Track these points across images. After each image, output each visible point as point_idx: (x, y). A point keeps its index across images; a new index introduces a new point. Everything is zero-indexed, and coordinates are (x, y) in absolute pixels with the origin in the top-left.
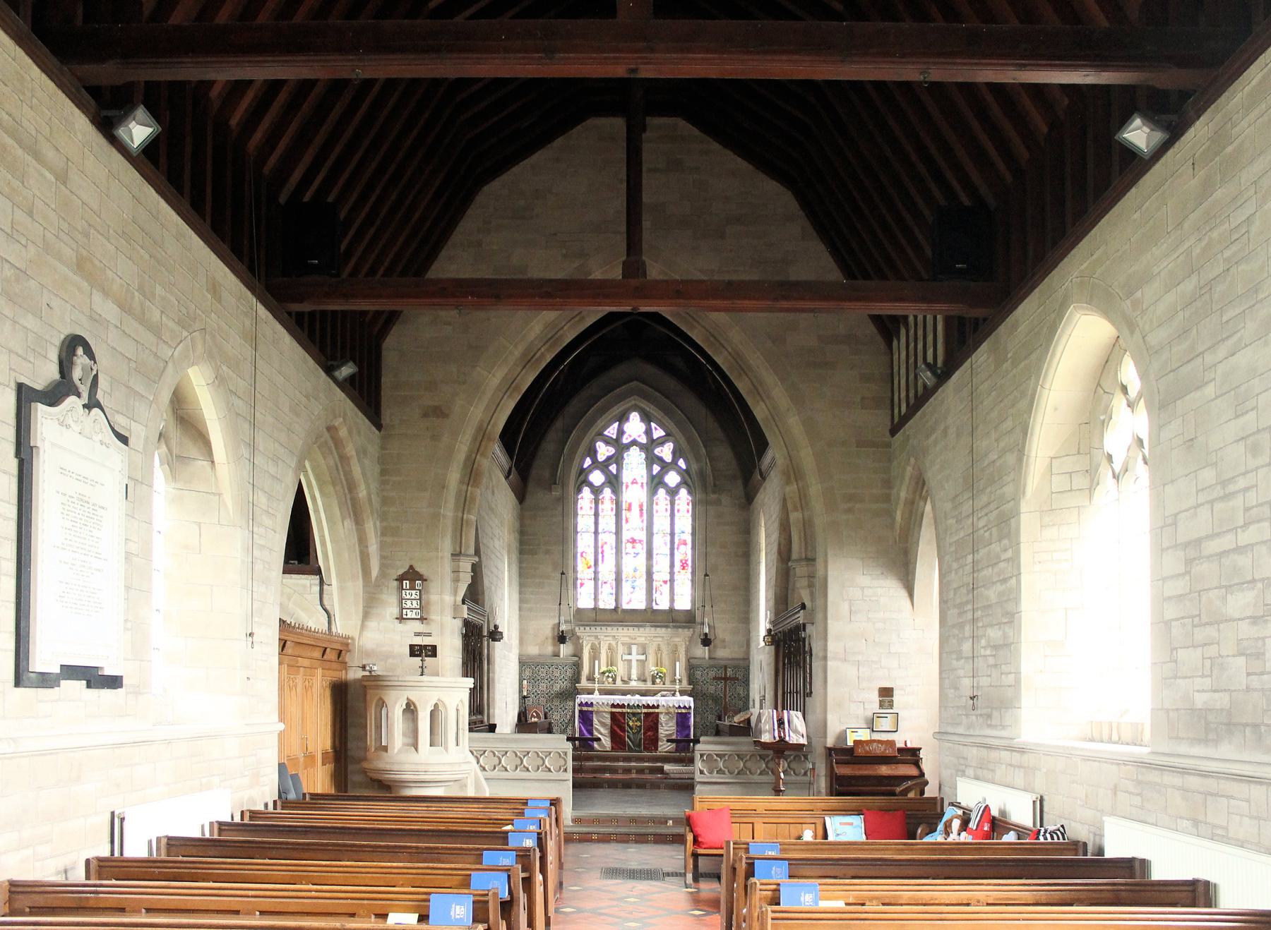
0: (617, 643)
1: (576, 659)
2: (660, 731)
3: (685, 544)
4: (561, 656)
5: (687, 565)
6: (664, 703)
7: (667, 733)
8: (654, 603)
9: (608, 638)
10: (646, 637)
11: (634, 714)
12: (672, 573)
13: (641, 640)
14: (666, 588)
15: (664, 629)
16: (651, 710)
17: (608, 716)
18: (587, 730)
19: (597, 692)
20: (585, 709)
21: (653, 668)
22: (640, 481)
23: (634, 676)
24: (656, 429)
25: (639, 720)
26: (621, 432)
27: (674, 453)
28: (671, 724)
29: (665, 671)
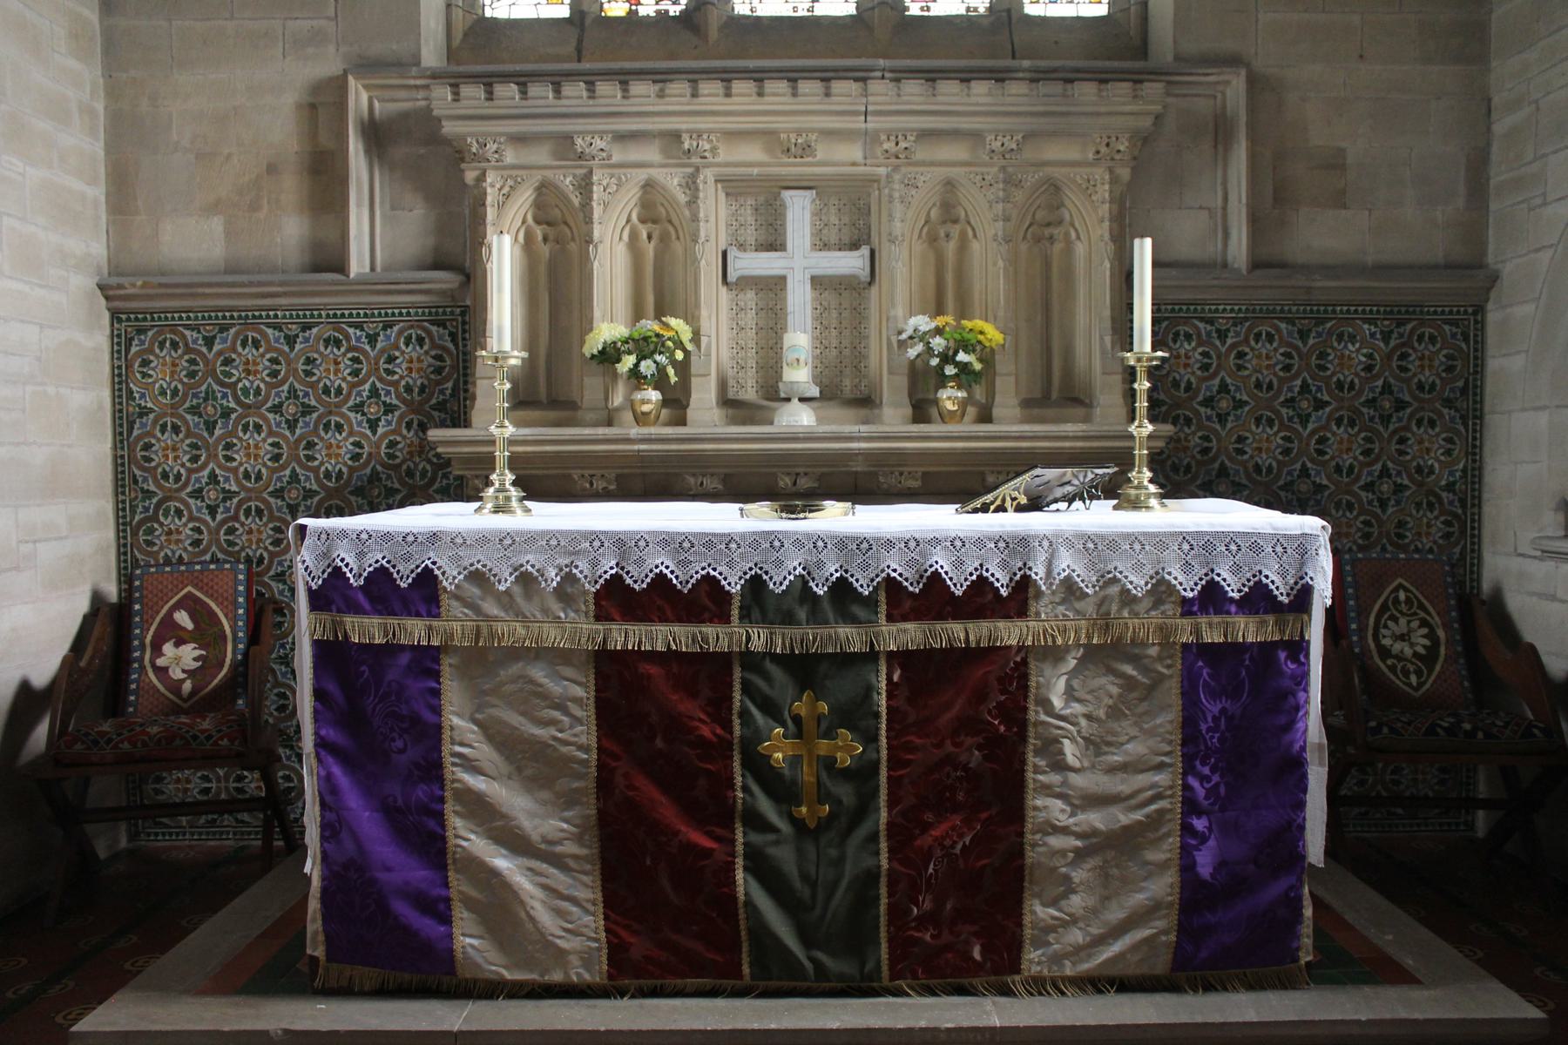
0: (691, 185)
1: (445, 280)
2: (1046, 808)
4: (358, 265)
6: (1067, 563)
9: (635, 153)
10: (870, 139)
13: (845, 157)
16: (958, 632)
17: (578, 689)
18: (392, 814)
19: (503, 477)
20: (367, 628)
21: (923, 323)
23: (799, 376)
25: (854, 715)
28: (1136, 749)
29: (993, 334)
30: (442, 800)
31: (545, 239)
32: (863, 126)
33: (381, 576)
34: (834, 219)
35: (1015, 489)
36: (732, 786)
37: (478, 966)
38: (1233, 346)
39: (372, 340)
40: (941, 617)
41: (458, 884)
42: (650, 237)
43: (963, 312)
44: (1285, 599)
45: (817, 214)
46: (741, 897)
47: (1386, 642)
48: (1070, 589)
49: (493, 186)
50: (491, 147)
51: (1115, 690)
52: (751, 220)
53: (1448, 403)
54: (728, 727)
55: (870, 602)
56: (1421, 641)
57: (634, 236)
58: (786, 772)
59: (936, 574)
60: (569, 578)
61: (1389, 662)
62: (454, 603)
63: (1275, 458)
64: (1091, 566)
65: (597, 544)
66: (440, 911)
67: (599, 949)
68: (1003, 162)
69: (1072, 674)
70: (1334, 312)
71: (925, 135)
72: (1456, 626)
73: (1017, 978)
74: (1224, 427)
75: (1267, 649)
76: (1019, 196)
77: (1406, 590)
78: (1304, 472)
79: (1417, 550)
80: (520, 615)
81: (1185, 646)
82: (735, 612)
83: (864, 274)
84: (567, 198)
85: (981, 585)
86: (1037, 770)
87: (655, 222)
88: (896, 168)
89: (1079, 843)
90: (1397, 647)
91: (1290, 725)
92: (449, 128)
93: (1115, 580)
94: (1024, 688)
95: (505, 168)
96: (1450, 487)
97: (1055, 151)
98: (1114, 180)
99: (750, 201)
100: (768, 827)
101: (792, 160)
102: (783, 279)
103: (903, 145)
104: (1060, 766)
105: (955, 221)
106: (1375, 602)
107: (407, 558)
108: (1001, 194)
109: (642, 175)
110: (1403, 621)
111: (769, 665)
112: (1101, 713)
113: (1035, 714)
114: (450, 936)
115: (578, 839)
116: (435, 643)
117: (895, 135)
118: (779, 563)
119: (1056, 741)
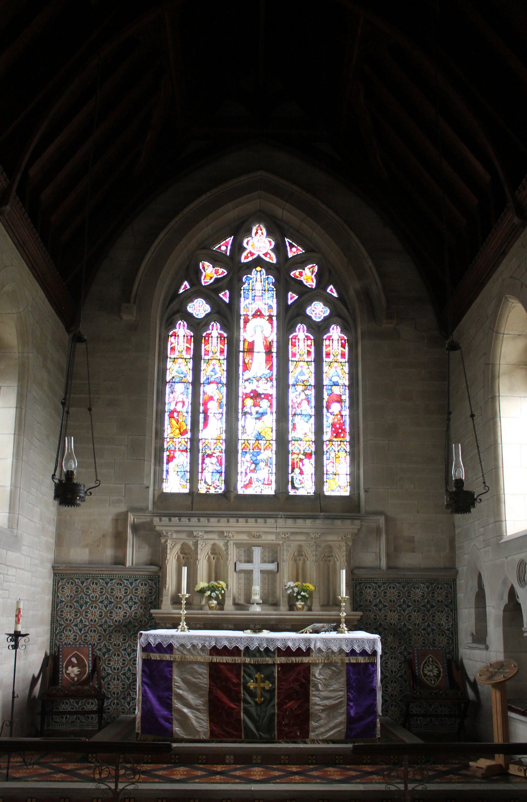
0: (226, 545)
1: (154, 568)
2: (314, 699)
3: (340, 400)
4: (128, 564)
5: (344, 430)
6: (319, 645)
7: (327, 702)
8: (290, 486)
9: (210, 536)
10: (277, 534)
11: (258, 667)
12: (319, 442)
13: (270, 538)
14: (309, 466)
15: (309, 522)
17: (205, 671)
18: (160, 699)
19: (183, 624)
20: (156, 656)
22: (266, 313)
24: (291, 246)
25: (269, 678)
26: (238, 248)
27: (319, 277)
30: (172, 696)
31: (183, 558)
32: (275, 531)
33: (159, 645)
34: (267, 554)
35: (309, 628)
36: (240, 693)
37: (178, 734)
38: (383, 590)
39: (131, 584)
40: (290, 656)
41: (175, 715)
42: (214, 558)
43: (304, 581)
44: (370, 653)
45: (262, 553)
46: (242, 719)
47: (426, 672)
48: (320, 650)
49: (169, 544)
50: (170, 533)
51: (330, 673)
52: (243, 554)
53: (447, 606)
54: (240, 680)
55: (273, 653)
56: (435, 672)
57: (209, 558)
58: (253, 690)
59: (289, 646)
60: (204, 646)
61: (426, 678)
62: (177, 651)
63: (396, 621)
64: (325, 645)
65: (211, 638)
66: (170, 721)
67: (208, 731)
68: (315, 540)
69: (320, 669)
70: (412, 580)
71: (293, 533)
72: (446, 668)
73: (308, 739)
74: (381, 613)
75: (366, 664)
76: (320, 549)
77: (432, 658)
78: (405, 625)
79: (439, 647)
80: (192, 654)
81: (347, 663)
82: (242, 654)
83: (276, 570)
84: (191, 548)
85: (299, 649)
86: (312, 691)
87: (215, 554)
88: (285, 542)
89: (322, 708)
90: (429, 674)
91: (372, 682)
92: (158, 528)
93: (330, 648)
94: (309, 672)
95: (173, 539)
96: (448, 629)
97: (330, 538)
98: (347, 545)
99: (243, 549)
100: (249, 703)
101: (255, 539)
102: (252, 570)
103: (287, 536)
104: (318, 690)
105: (302, 555)
106: (423, 661)
107: (166, 641)
108: (315, 549)
109: (212, 542)
110: (431, 666)
111: (250, 666)
112: (328, 678)
113: (312, 678)
114: (172, 727)
115: (204, 705)
116: (172, 660)
117: (285, 533)
118: (253, 644)
119: (317, 684)
